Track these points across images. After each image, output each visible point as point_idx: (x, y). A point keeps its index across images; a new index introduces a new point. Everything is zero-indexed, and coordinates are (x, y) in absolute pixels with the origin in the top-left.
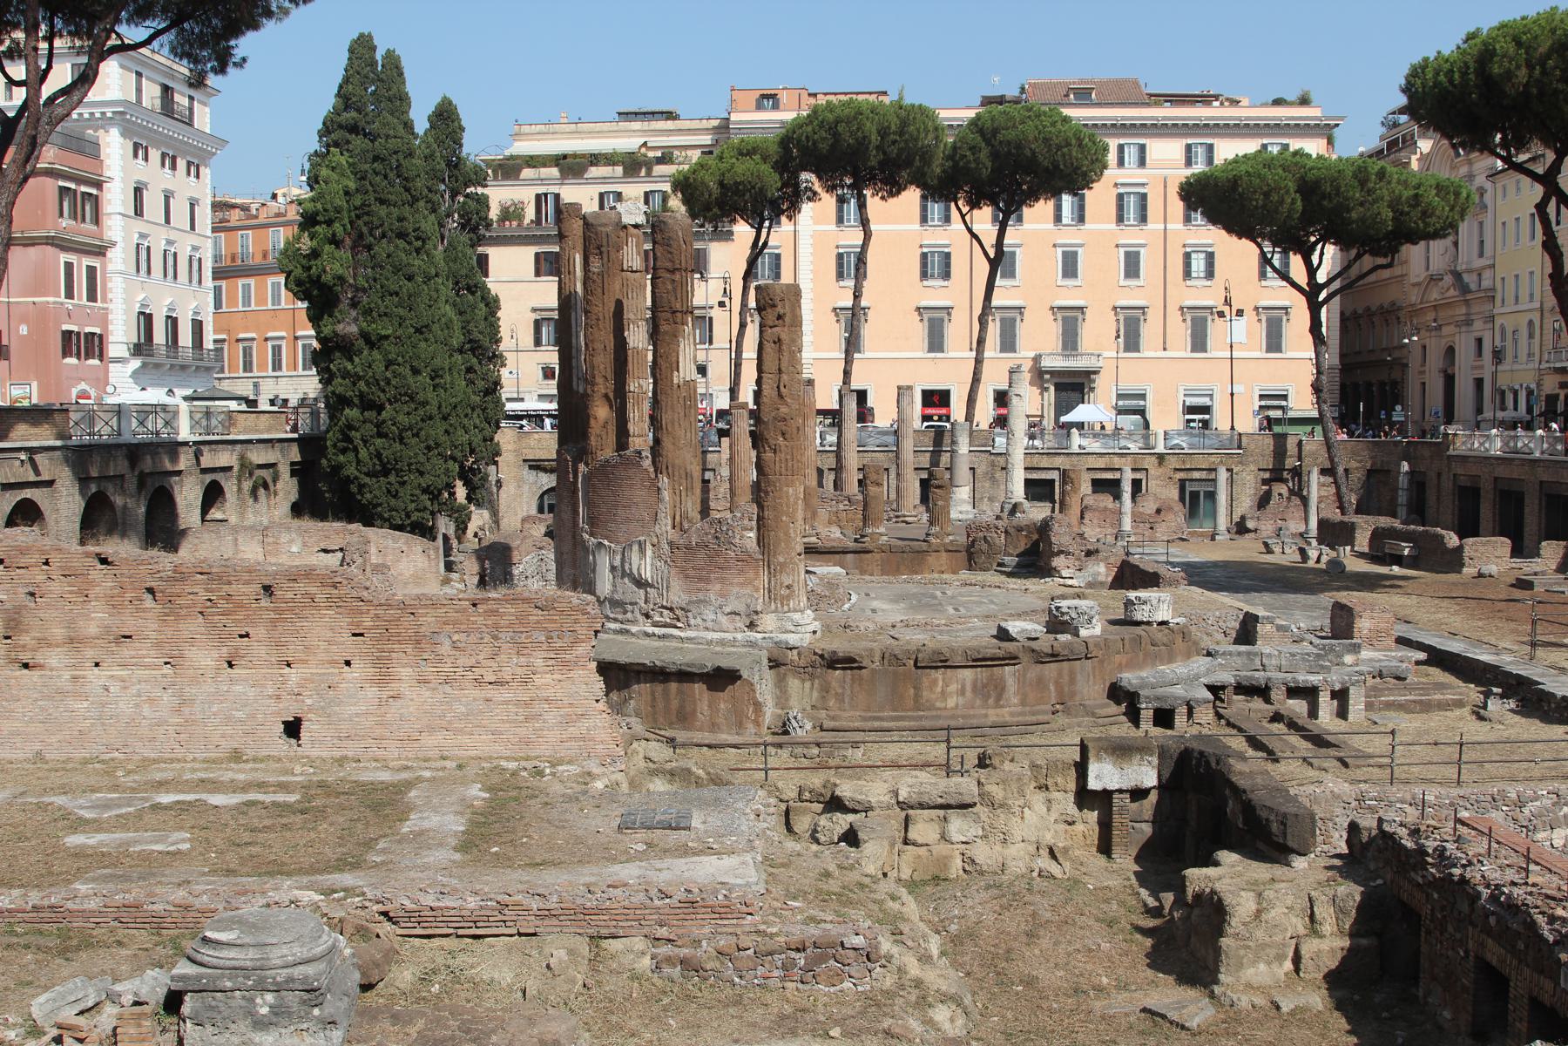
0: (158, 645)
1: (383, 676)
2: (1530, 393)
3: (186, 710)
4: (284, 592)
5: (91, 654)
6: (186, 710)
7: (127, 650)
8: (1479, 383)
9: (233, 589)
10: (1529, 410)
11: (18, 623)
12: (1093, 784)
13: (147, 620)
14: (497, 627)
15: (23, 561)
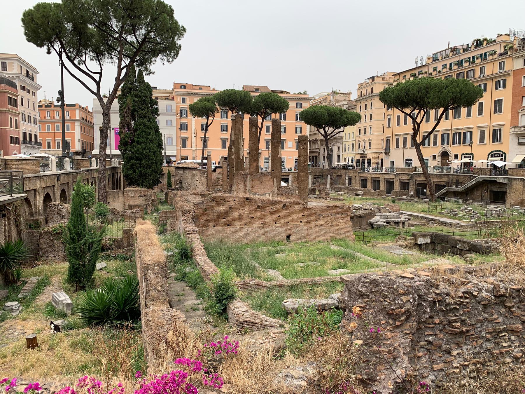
0: (260, 219)
1: (308, 225)
2: (352, 159)
3: (266, 234)
4: (289, 206)
5: (244, 221)
6: (266, 234)
7: (253, 221)
8: (339, 156)
9: (277, 206)
10: (352, 162)
11: (227, 215)
12: (419, 243)
13: (258, 214)
14: (332, 212)
15: (229, 200)
